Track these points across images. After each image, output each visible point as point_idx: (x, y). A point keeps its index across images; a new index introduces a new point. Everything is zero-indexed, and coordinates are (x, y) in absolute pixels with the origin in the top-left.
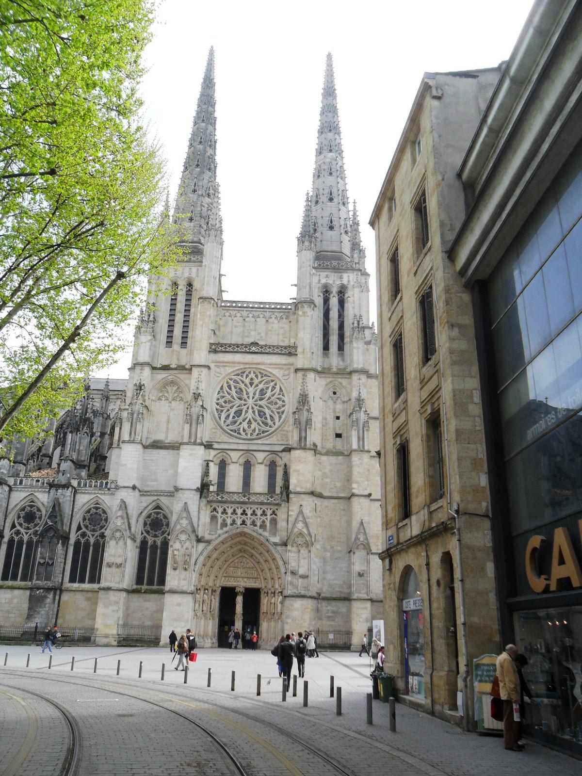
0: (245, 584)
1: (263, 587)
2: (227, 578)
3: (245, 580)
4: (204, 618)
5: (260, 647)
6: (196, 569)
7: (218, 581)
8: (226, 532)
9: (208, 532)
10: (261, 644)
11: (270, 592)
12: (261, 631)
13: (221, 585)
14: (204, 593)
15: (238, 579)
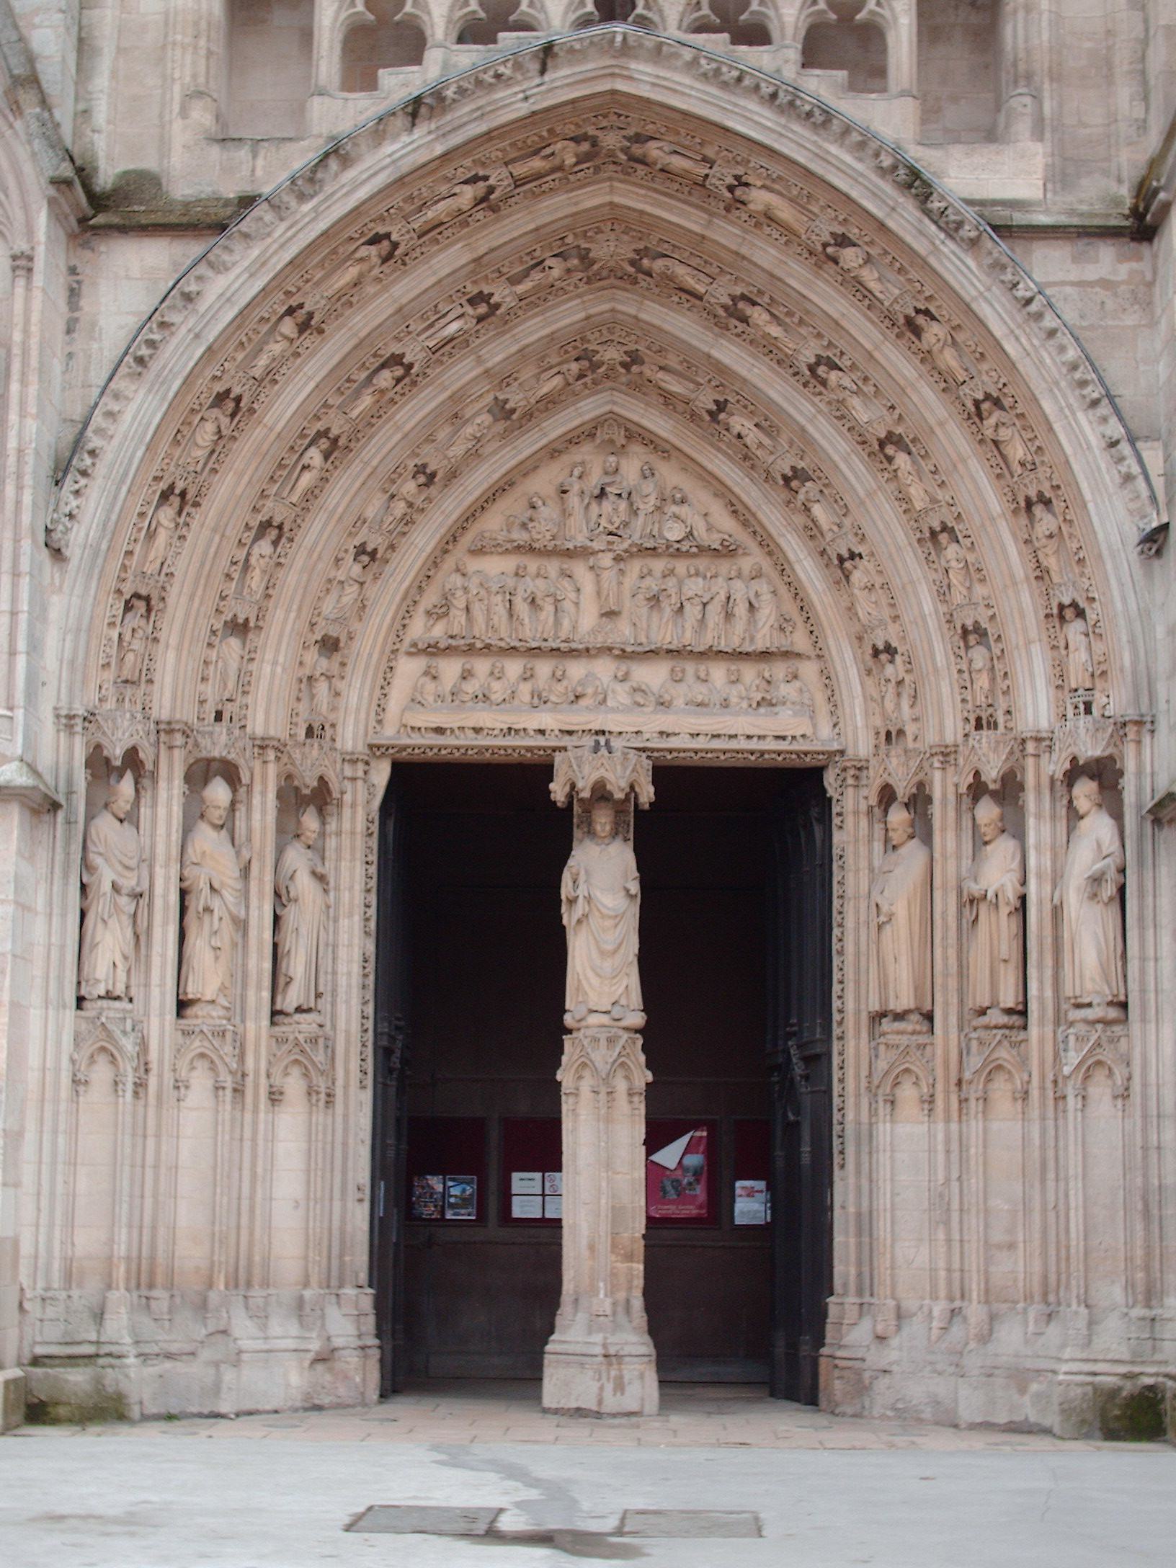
0: (665, 721)
1: (861, 744)
2: (450, 669)
3: (653, 675)
4: (200, 1082)
5: (861, 1389)
6: (77, 539)
7: (356, 692)
8: (415, 109)
9: (202, 116)
10: (876, 1358)
11: (945, 786)
12: (865, 1224)
13: (389, 734)
14: (194, 814)
15: (576, 670)
